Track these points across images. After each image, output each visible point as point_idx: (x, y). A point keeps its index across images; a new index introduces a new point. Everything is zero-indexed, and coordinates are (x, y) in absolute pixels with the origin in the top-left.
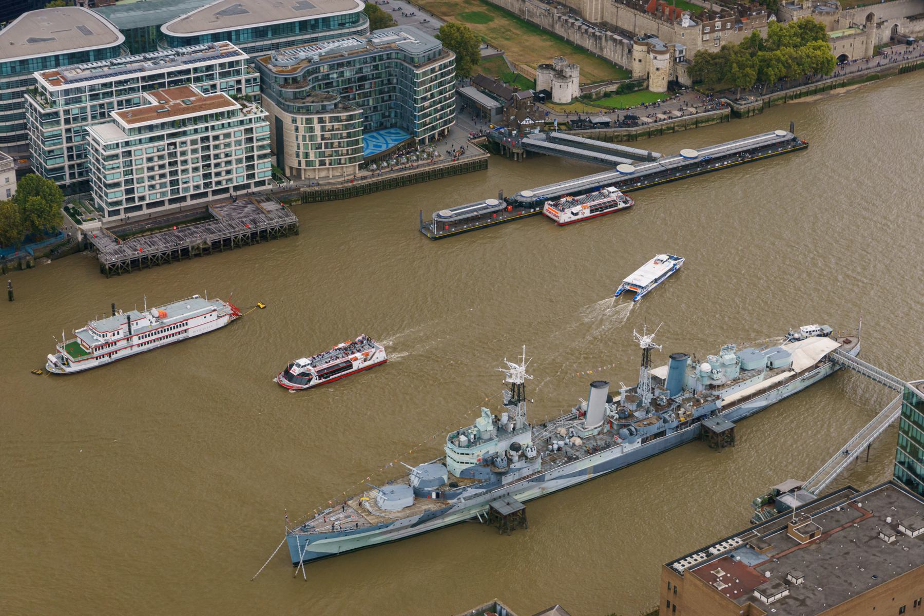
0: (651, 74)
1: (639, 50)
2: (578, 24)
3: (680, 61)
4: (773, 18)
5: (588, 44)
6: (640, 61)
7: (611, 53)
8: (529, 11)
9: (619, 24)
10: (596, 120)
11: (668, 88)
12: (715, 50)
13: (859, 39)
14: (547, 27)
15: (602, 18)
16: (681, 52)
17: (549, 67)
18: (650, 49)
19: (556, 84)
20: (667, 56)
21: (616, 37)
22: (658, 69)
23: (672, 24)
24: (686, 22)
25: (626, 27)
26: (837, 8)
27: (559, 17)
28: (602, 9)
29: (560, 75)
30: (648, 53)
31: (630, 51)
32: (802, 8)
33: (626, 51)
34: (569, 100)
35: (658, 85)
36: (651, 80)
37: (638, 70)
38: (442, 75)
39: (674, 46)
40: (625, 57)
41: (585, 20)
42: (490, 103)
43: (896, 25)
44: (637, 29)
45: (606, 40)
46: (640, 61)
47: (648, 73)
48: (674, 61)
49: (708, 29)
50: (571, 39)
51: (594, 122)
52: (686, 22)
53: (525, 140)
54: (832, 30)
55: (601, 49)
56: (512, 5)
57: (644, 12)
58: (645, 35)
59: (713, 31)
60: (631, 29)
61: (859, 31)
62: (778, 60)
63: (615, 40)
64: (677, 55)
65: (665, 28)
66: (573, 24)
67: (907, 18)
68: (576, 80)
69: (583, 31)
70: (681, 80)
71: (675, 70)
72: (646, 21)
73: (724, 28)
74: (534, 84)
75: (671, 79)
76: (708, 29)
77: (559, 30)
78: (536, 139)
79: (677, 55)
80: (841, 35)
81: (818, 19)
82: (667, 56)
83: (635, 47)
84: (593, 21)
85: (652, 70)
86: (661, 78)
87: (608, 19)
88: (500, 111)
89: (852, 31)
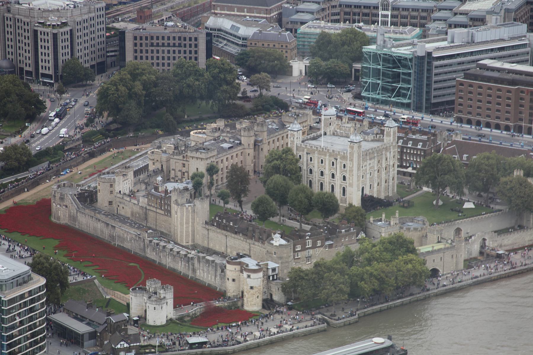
0: (245, 293)
1: (231, 270)
2: (170, 246)
3: (273, 280)
4: (362, 235)
5: (180, 267)
6: (234, 280)
7: (205, 275)
8: (119, 237)
9: (211, 246)
11: (264, 307)
12: (307, 266)
13: (448, 254)
14: (138, 251)
15: (193, 240)
16: (274, 270)
19: (150, 307)
20: (261, 274)
21: (208, 258)
22: (252, 288)
23: (263, 243)
25: (217, 248)
26: (424, 224)
27: (151, 241)
28: (193, 231)
30: (242, 271)
31: (223, 271)
32: (390, 224)
33: (219, 271)
34: (164, 322)
36: (245, 299)
38: (32, 301)
39: (267, 264)
40: (218, 278)
41: (176, 243)
42: (81, 328)
43: (484, 240)
44: (229, 250)
45: (199, 261)
46: (234, 280)
47: (243, 292)
49: (299, 248)
50: (164, 262)
51: (190, 342)
54: (421, 245)
55: (194, 271)
56: (102, 232)
57: (236, 233)
58: (238, 254)
59: (304, 249)
60: (223, 250)
61: (448, 245)
62: (371, 275)
63: (208, 261)
64: (270, 273)
65: (257, 247)
66: (164, 247)
67: (495, 232)
68: (171, 302)
69: (175, 253)
70: (276, 298)
71: (269, 288)
72: (237, 242)
73: (314, 247)
74: (127, 308)
75: (265, 297)
76: (299, 248)
79: (270, 273)
80: (430, 249)
81: (408, 235)
82: (261, 274)
83: (228, 267)
84: (184, 244)
85: (246, 288)
86: (255, 296)
87: (199, 241)
88: (93, 335)
89: (441, 246)
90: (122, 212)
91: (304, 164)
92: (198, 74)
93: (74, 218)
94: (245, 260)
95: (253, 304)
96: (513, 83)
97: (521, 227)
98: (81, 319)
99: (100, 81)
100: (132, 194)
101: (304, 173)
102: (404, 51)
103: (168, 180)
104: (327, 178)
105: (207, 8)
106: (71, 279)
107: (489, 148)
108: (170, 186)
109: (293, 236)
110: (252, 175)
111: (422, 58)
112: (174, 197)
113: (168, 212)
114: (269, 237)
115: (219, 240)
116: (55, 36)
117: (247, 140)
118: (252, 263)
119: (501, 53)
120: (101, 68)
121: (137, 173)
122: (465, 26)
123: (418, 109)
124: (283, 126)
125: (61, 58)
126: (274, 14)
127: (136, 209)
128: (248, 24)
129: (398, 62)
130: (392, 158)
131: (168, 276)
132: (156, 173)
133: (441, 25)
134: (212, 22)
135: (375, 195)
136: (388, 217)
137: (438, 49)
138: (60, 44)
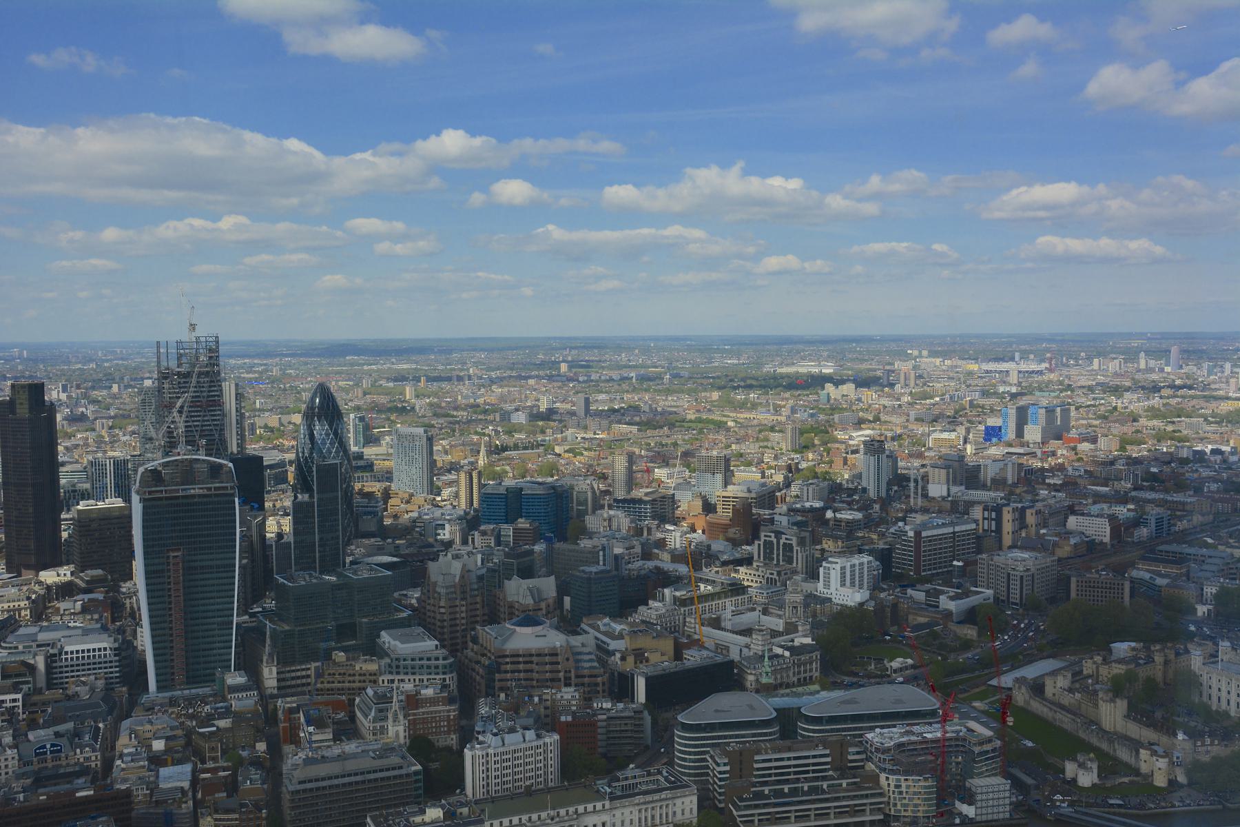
5: (1104, 746)
7: (1124, 754)
9: (1128, 733)
12: (1206, 759)
17: (1074, 760)
18: (1154, 753)
19: (1081, 772)
24: (1180, 736)
29: (1082, 766)
35: (1160, 781)
37: (1144, 768)
49: (1199, 743)
52: (1180, 736)
55: (1115, 750)
59: (1203, 745)
65: (1164, 739)
68: (1095, 771)
73: (1212, 744)
74: (1063, 771)
76: (1199, 743)
85: (1156, 769)
87: (1119, 728)
94: (1155, 748)
100: (1070, 690)
101: (1205, 688)
103: (1097, 683)
105: (1132, 565)
108: (1097, 687)
112: (1101, 695)
114: (1175, 735)
115: (1134, 730)
117: (1158, 658)
118: (1160, 751)
124: (1187, 651)
126: (1184, 570)
127: (1072, 701)
132: (1089, 676)
134: (1134, 573)
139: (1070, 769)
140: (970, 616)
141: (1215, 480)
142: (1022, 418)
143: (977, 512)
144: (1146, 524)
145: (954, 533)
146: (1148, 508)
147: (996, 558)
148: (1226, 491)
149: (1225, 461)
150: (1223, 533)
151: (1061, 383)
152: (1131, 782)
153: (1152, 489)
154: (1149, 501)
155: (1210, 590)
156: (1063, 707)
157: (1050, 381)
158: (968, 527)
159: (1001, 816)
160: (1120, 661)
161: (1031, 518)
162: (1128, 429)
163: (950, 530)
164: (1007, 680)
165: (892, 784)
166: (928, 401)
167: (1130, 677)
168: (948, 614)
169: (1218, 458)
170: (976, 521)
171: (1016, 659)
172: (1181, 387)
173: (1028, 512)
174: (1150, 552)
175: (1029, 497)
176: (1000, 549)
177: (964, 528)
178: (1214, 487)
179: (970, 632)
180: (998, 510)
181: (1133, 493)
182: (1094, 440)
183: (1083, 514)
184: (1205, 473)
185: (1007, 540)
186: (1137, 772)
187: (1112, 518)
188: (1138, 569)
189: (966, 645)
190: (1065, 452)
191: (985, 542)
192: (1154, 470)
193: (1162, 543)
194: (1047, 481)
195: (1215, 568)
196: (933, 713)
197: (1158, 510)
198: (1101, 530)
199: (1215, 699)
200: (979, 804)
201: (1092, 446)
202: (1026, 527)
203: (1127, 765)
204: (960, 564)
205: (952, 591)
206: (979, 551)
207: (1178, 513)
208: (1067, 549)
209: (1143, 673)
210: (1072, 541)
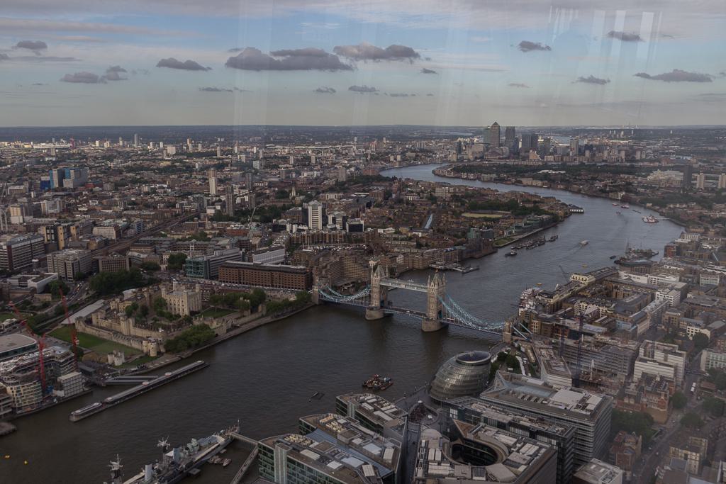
5: (126, 343)
7: (135, 345)
10: (133, 369)
12: (172, 338)
17: (112, 353)
19: (116, 359)
35: (153, 354)
37: (145, 350)
48: (159, 344)
53: (107, 381)
59: (171, 332)
60: (140, 335)
68: (123, 356)
77: (114, 340)
78: (111, 380)
81: (206, 323)
87: (133, 333)
88: (95, 372)
90: (102, 325)
91: (168, 301)
92: (127, 272)
93: (84, 330)
95: (153, 354)
96: (237, 268)
97: (244, 316)
98: (90, 366)
99: (90, 278)
101: (168, 305)
102: (200, 260)
104: (177, 306)
105: (128, 249)
106: (85, 352)
107: (231, 291)
108: (119, 314)
109: (166, 328)
110: (149, 308)
111: (206, 261)
112: (121, 318)
113: (120, 324)
114: (158, 330)
116: (73, 264)
118: (152, 339)
119: (233, 258)
120: (91, 273)
121: (106, 311)
122: (219, 250)
123: (207, 279)
124: (159, 289)
125: (75, 272)
127: (108, 324)
128: (142, 253)
129: (198, 263)
130: (199, 297)
131: (122, 348)
132: (114, 310)
133: (211, 250)
134: (130, 254)
135: (194, 310)
136: (200, 318)
137: (212, 258)
138: (75, 267)
139: (110, 358)
140: (46, 289)
141: (163, 203)
142: (62, 176)
143: (43, 230)
144: (132, 227)
145: (31, 244)
146: (133, 219)
147: (57, 255)
148: (168, 207)
149: (165, 192)
150: (168, 228)
151: (80, 154)
152: (141, 357)
153: (133, 209)
154: (132, 215)
155: (166, 257)
156: (103, 328)
157: (74, 154)
158: (39, 240)
159: (78, 392)
160: (129, 300)
161: (73, 231)
162: (118, 179)
163: (29, 242)
164: (72, 319)
165: (15, 391)
166: (3, 167)
167: (135, 307)
168: (34, 290)
169: (162, 190)
170: (42, 236)
171: (76, 307)
172: (141, 155)
173: (72, 227)
174: (136, 243)
175: (70, 219)
176: (58, 249)
177: (36, 240)
178: (162, 205)
179: (48, 297)
180: (55, 229)
181: (125, 212)
182: (101, 186)
183: (101, 226)
184: (157, 198)
185: (62, 244)
186: (142, 351)
187: (116, 227)
188: (132, 251)
189: (46, 305)
190: (87, 193)
191: (51, 247)
192: (133, 199)
193: (142, 236)
194: (79, 209)
195: (167, 246)
196: (34, 347)
197: (138, 220)
198: (110, 233)
199: (173, 309)
200: (66, 389)
201: (100, 189)
202: (71, 236)
203: (137, 350)
204: (36, 261)
205: (34, 277)
206: (46, 252)
207: (147, 220)
208: (95, 245)
209: (140, 304)
210: (97, 241)
